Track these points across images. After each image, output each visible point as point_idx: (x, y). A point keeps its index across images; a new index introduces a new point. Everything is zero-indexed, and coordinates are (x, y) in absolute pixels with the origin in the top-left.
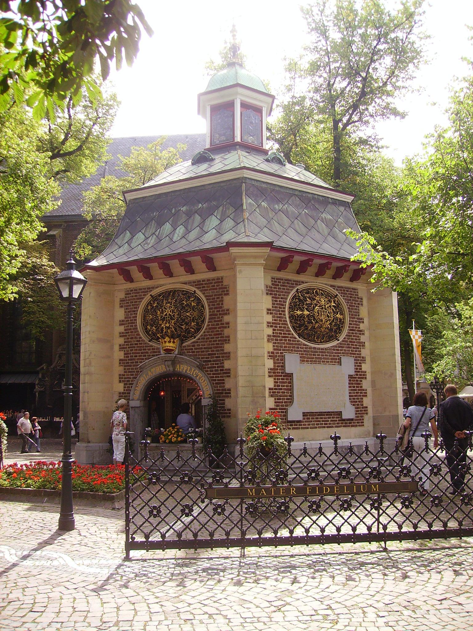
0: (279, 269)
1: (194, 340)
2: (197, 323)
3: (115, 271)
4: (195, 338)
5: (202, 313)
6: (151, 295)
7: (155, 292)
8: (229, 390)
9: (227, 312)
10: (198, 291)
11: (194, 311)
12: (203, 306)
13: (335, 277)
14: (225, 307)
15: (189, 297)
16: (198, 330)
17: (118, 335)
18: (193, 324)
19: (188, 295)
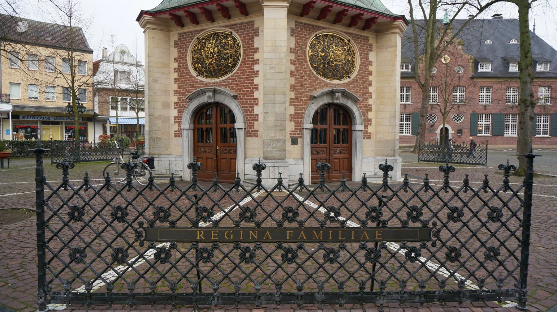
0: (302, 15)
1: (231, 74)
2: (234, 59)
3: (166, 16)
4: (232, 73)
5: (237, 51)
6: (197, 38)
7: (201, 35)
8: (257, 115)
9: (257, 50)
10: (234, 32)
11: (231, 48)
12: (238, 45)
13: (350, 26)
14: (256, 46)
15: (227, 38)
16: (234, 65)
17: (173, 71)
18: (230, 60)
19: (226, 36)
